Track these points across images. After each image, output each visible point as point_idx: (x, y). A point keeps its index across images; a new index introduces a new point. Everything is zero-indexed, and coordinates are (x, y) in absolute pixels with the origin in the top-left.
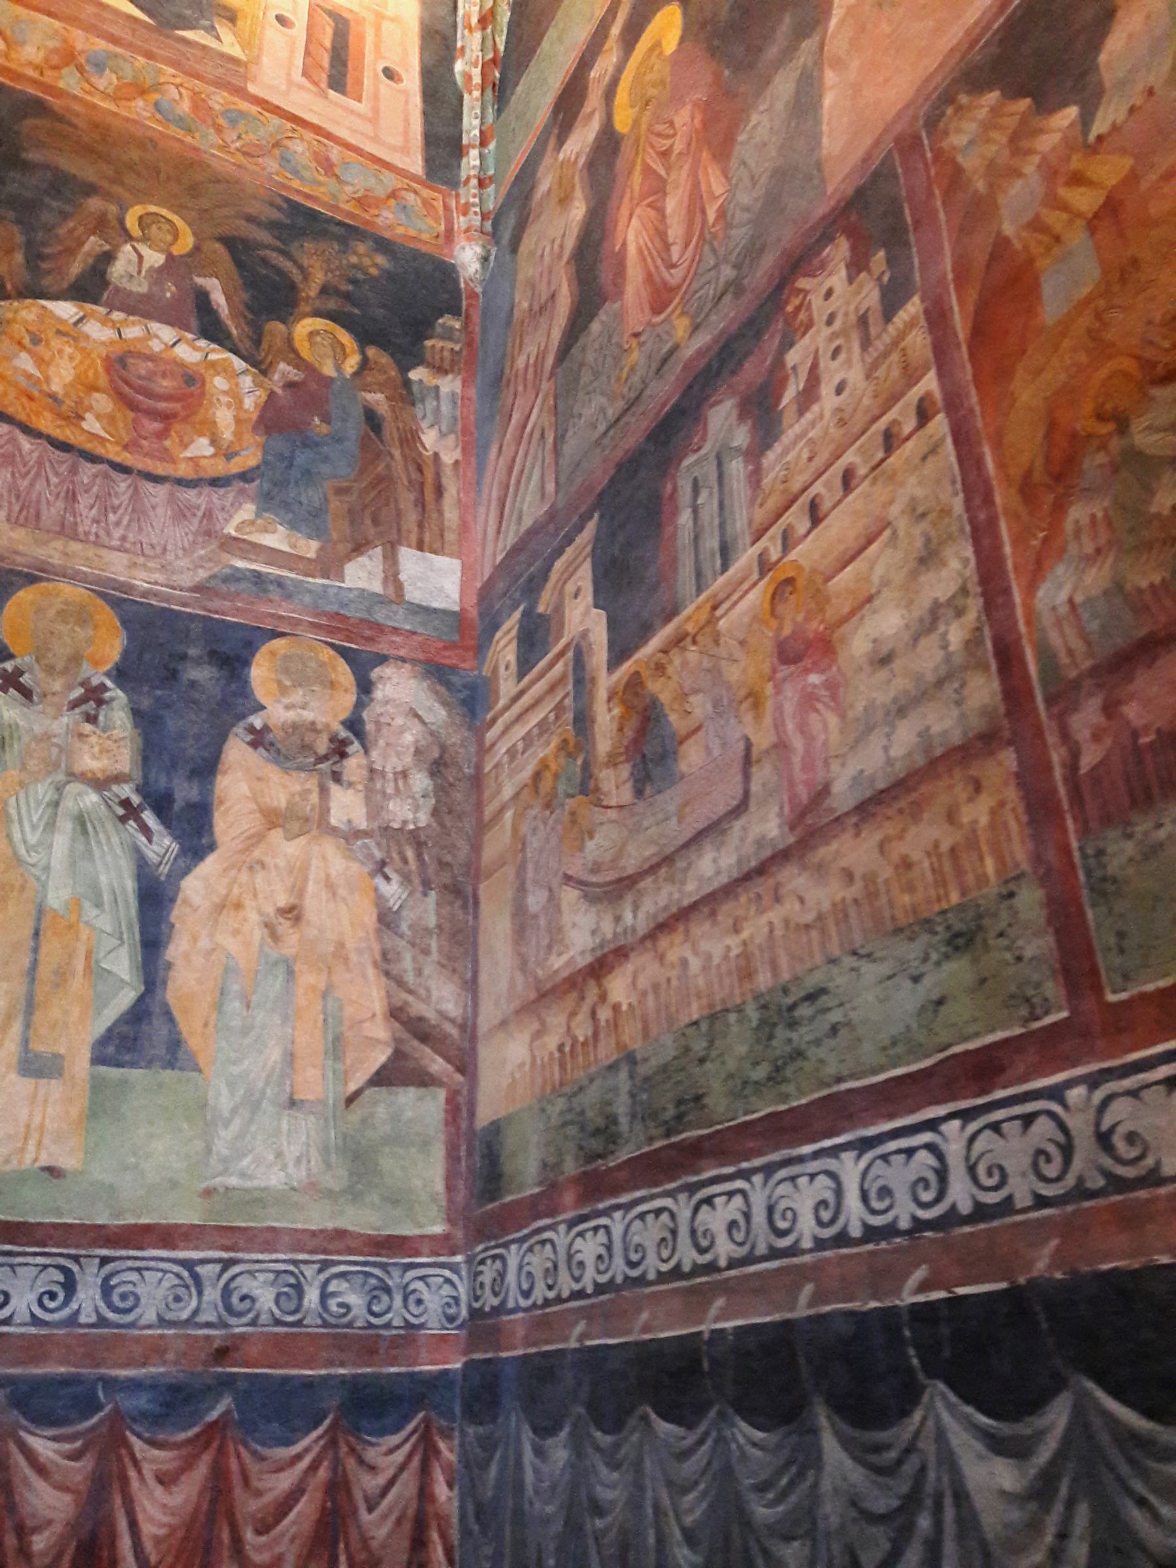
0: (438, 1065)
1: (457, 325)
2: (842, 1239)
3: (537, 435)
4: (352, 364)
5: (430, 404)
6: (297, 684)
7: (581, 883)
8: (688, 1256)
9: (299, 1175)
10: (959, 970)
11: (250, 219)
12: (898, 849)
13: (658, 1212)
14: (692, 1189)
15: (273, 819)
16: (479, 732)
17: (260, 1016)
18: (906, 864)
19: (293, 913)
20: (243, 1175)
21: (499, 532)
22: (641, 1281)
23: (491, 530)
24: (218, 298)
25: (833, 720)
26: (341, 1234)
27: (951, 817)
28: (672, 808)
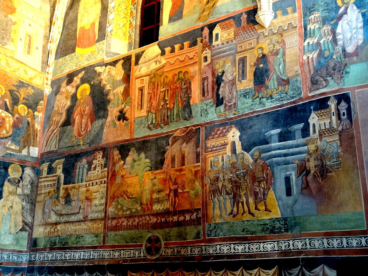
0: (28, 228)
1: (43, 103)
2: (80, 259)
3: (56, 135)
4: (26, 112)
5: (37, 119)
6: (14, 171)
7: (55, 212)
8: (63, 258)
9: (10, 242)
10: (95, 239)
11: (13, 85)
12: (93, 226)
13: (60, 253)
14: (65, 252)
15: (10, 193)
16: (39, 178)
17: (7, 222)
18: (93, 227)
19: (11, 207)
20: (4, 242)
21: (46, 146)
22: (57, 260)
23: (45, 144)
24: (8, 103)
25: (90, 209)
26: (14, 250)
27: (98, 225)
28: (70, 208)
